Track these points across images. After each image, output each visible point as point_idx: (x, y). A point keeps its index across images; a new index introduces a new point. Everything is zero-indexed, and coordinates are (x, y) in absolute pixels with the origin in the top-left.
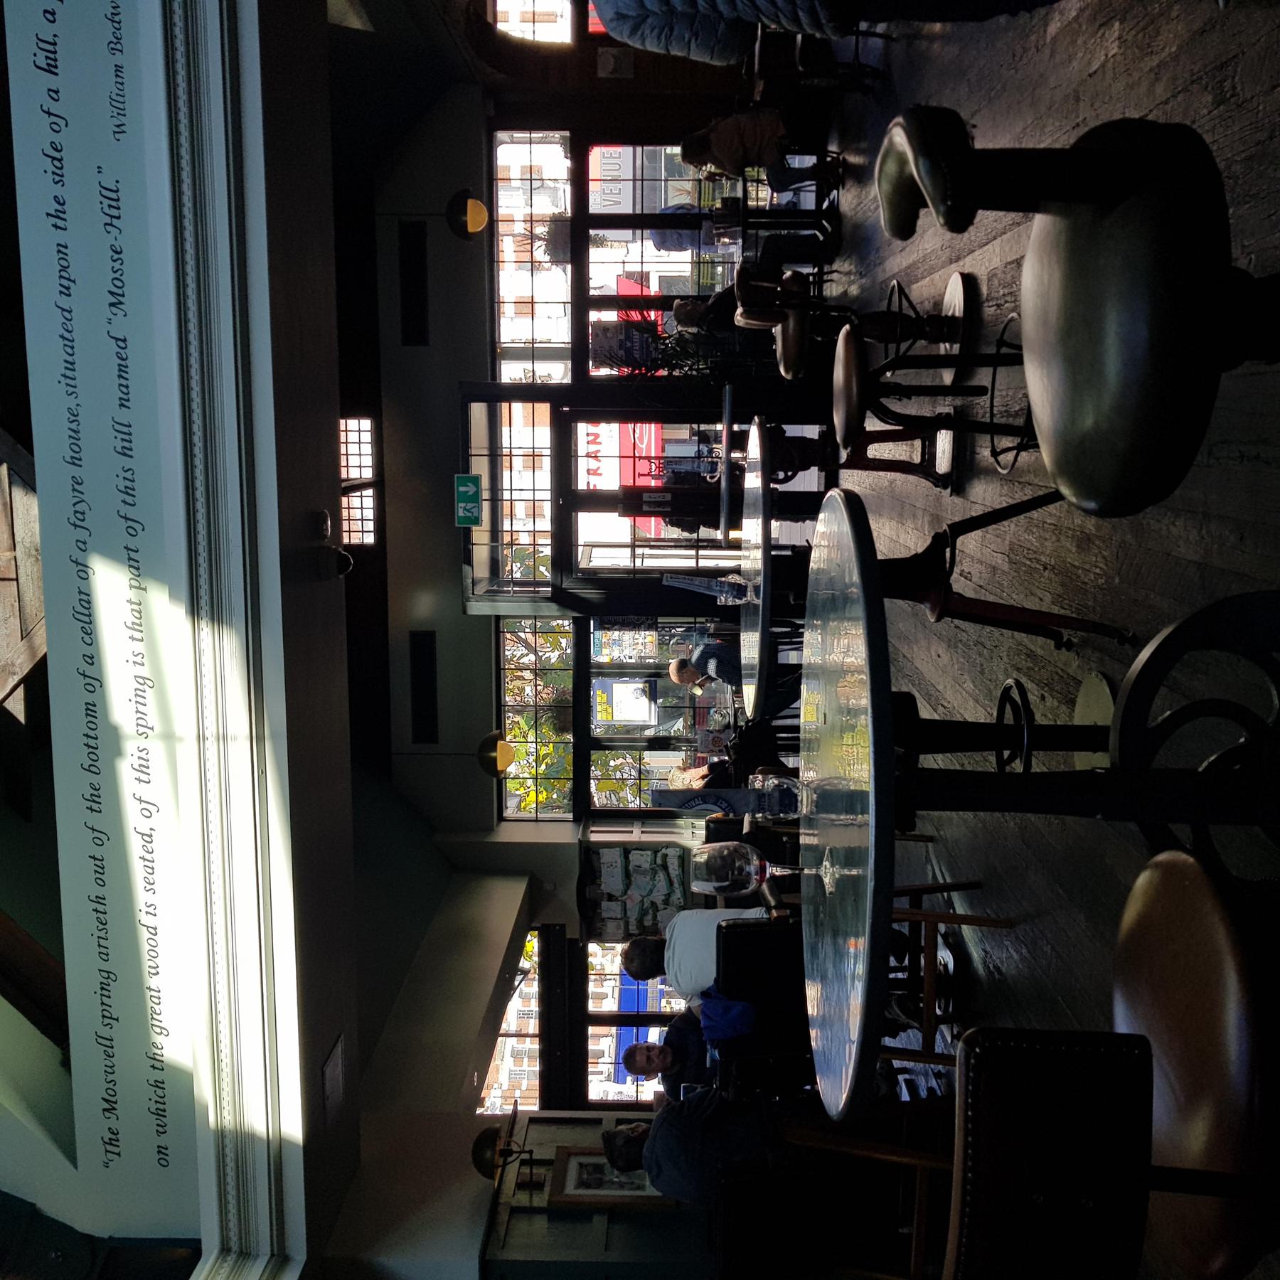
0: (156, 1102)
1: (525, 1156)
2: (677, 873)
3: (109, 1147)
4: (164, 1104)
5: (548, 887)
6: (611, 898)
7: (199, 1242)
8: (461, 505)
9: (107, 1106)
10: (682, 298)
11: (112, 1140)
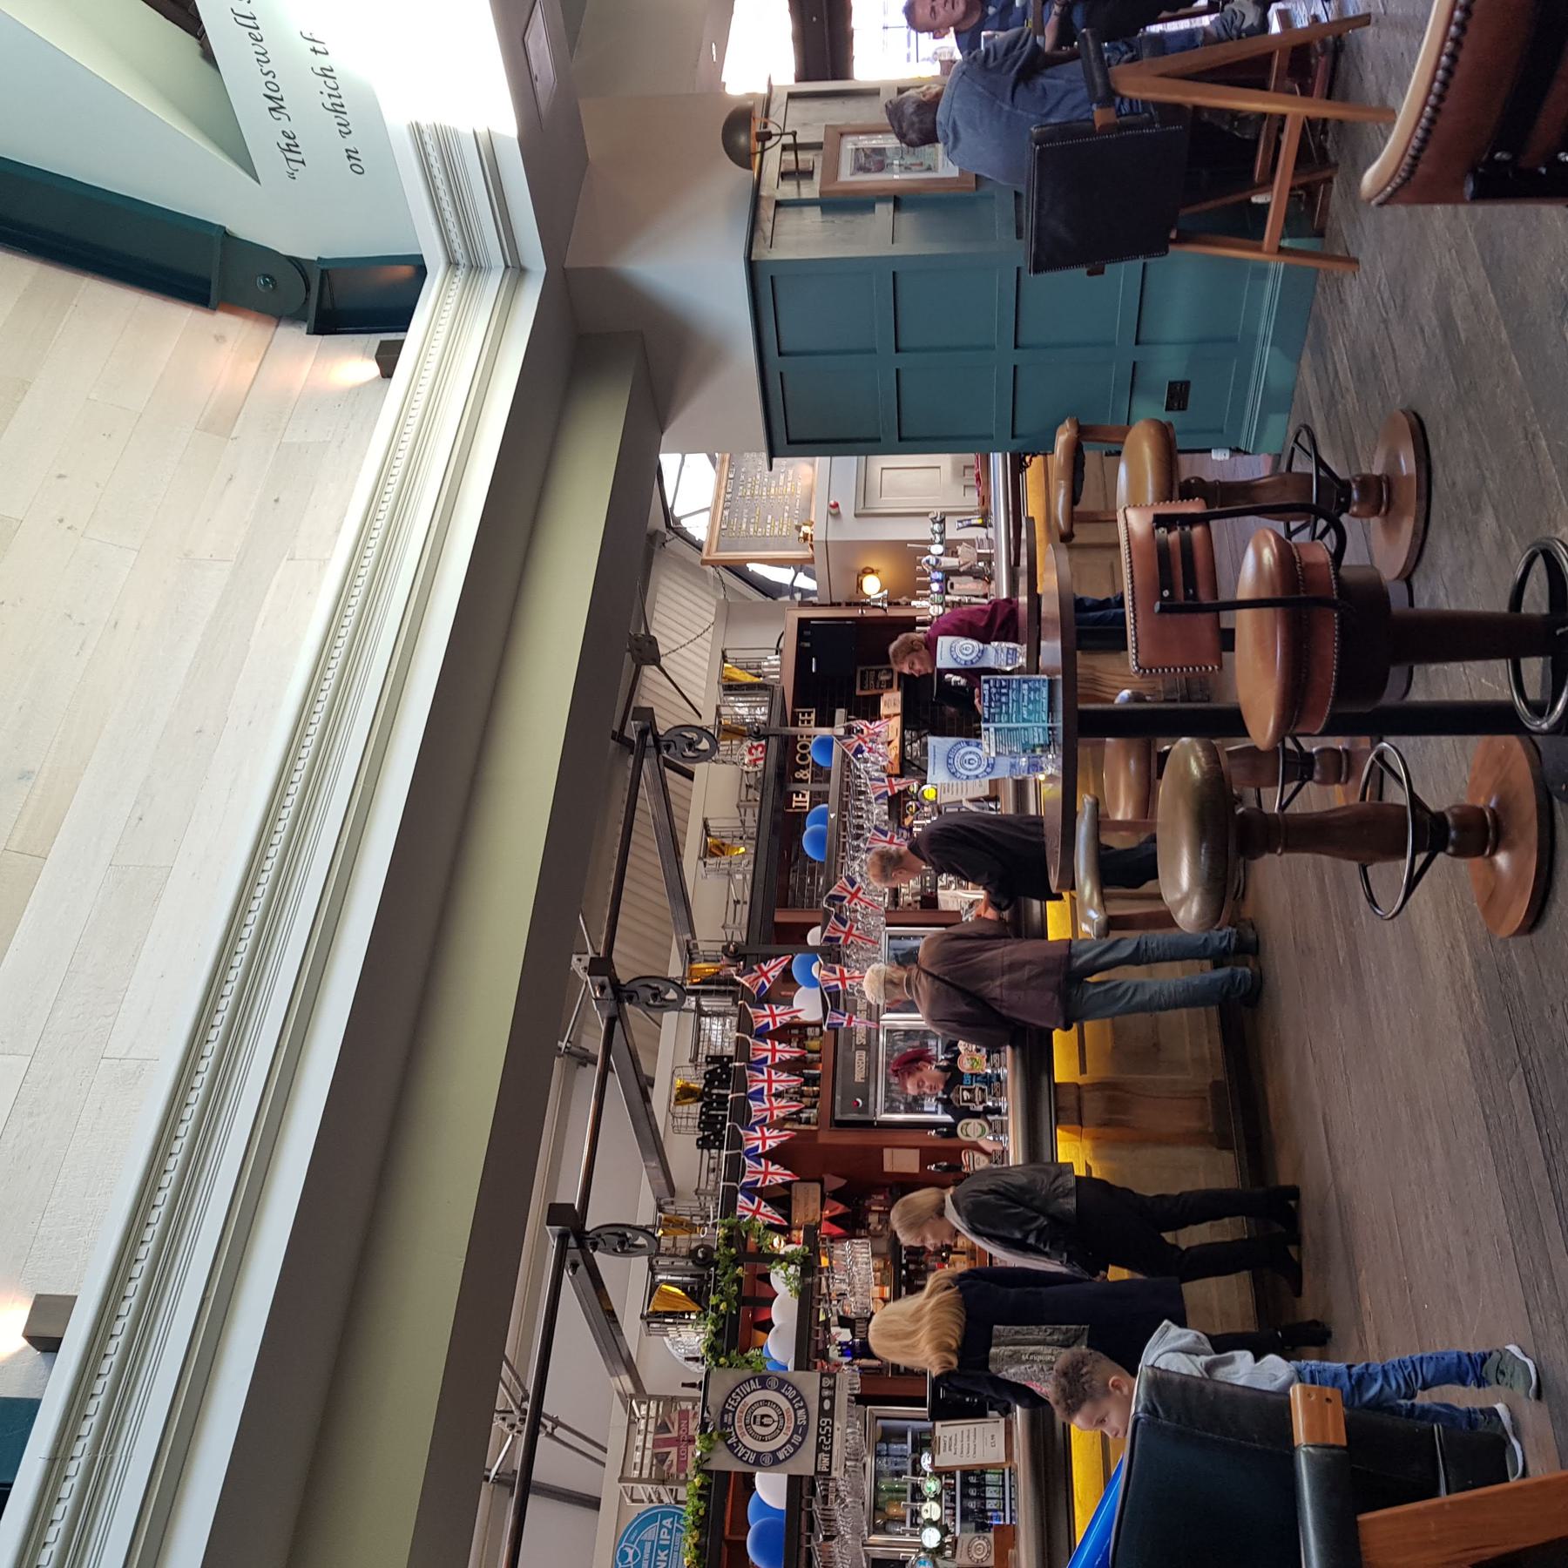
0: (330, 95)
1: (788, 140)
3: (289, 155)
4: (340, 97)
7: (422, 256)
9: (273, 105)
11: (291, 147)
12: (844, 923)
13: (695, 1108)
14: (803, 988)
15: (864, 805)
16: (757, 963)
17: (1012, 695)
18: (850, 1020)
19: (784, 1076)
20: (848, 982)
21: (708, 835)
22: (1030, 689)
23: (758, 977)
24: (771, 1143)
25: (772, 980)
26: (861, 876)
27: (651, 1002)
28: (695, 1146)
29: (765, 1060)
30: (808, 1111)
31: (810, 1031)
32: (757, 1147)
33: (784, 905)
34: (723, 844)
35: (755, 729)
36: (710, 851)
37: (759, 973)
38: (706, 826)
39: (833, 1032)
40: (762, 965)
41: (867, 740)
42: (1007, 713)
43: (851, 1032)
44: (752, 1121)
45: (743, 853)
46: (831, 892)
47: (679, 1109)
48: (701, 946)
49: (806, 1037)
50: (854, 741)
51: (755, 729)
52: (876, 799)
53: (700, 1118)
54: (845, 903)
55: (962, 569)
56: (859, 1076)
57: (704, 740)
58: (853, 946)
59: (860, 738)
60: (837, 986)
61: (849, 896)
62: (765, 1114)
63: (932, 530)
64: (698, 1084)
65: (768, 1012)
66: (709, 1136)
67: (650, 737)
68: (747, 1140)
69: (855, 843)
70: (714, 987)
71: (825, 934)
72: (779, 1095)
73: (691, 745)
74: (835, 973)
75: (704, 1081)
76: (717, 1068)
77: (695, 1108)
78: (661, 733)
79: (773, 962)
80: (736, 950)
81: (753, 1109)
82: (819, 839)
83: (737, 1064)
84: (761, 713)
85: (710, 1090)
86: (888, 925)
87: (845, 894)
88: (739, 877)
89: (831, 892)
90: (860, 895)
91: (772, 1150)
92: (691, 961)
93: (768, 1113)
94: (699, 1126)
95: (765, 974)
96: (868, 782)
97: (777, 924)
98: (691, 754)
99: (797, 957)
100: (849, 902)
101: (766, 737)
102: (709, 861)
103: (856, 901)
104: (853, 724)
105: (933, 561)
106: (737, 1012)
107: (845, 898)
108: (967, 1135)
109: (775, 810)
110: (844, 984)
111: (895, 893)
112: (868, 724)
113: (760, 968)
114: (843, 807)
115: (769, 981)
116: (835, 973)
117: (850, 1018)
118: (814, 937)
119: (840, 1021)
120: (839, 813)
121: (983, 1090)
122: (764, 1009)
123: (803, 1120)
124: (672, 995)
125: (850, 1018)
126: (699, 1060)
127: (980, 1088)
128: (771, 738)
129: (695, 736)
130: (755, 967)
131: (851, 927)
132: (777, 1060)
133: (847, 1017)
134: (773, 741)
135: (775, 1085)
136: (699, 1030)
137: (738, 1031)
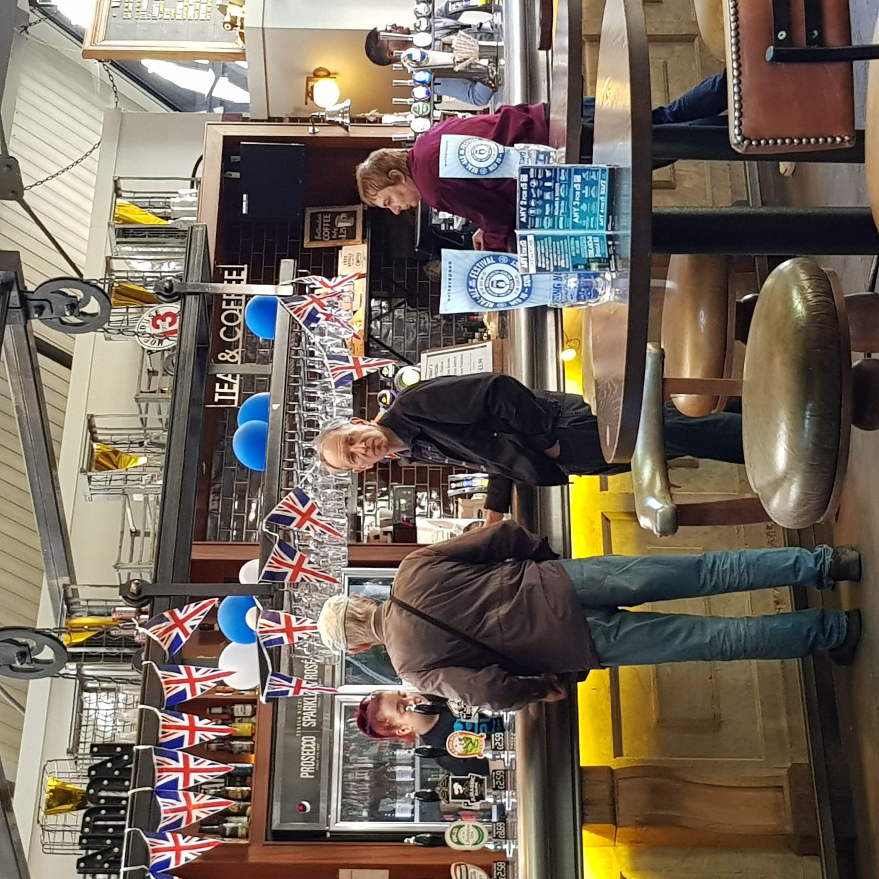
12: (291, 554)
13: (76, 818)
14: (234, 644)
15: (319, 394)
16: (170, 608)
17: (560, 191)
18: (298, 687)
19: (206, 764)
20: (296, 635)
21: (94, 439)
22: (584, 183)
23: (171, 628)
24: (188, 856)
25: (190, 631)
26: (316, 490)
27: (18, 664)
28: (76, 870)
29: (179, 741)
30: (234, 819)
31: (238, 709)
32: (167, 862)
33: (202, 536)
34: (116, 453)
35: (167, 284)
36: (98, 462)
37: (172, 622)
38: (91, 427)
39: (271, 704)
40: (177, 611)
41: (325, 302)
42: (552, 215)
43: (294, 704)
44: (161, 826)
45: (144, 466)
46: (274, 512)
47: (51, 820)
48: (84, 593)
49: (233, 718)
50: (307, 304)
51: (167, 284)
52: (337, 384)
53: (82, 832)
54: (293, 526)
55: (457, 69)
56: (305, 772)
57: (93, 300)
58: (303, 586)
59: (314, 300)
60: (281, 640)
61: (298, 518)
62: (180, 815)
63: (416, 12)
64: (80, 785)
65: (185, 676)
66: (95, 855)
67: (14, 293)
68: (155, 851)
69: (306, 445)
70: (103, 650)
71: (266, 569)
72: (197, 789)
73: (74, 306)
74: (279, 622)
75: (87, 781)
76: (106, 762)
77: (76, 818)
78: (31, 288)
79: (192, 608)
80: (139, 591)
81: (163, 808)
82: (257, 441)
83: (141, 747)
84: (172, 267)
85: (96, 792)
86: (351, 564)
87: (293, 514)
88: (138, 497)
89: (274, 512)
90: (314, 516)
91: (189, 866)
92: (70, 613)
93: (184, 814)
94: (80, 843)
95: (179, 624)
96: (326, 361)
97: (194, 562)
98: (74, 320)
99: (228, 598)
100: (299, 526)
101: (180, 297)
102: (97, 476)
103: (308, 523)
104: (305, 280)
105: (416, 55)
106: (141, 677)
107: (293, 519)
108: (459, 843)
109: (193, 402)
110: (290, 637)
111: (356, 523)
112: (326, 280)
113: (173, 615)
114: (291, 397)
115: (186, 633)
116: (279, 622)
117: (299, 683)
118: (250, 574)
119: (284, 689)
120: (285, 404)
121: (480, 782)
122: (180, 673)
123: (228, 832)
124: (47, 654)
125: (299, 683)
126: (81, 751)
127: (477, 780)
128: (188, 298)
129: (80, 294)
130: (167, 614)
131: (302, 559)
132: (197, 742)
133: (294, 684)
134: (192, 303)
135: (193, 776)
136: (81, 709)
137: (142, 703)
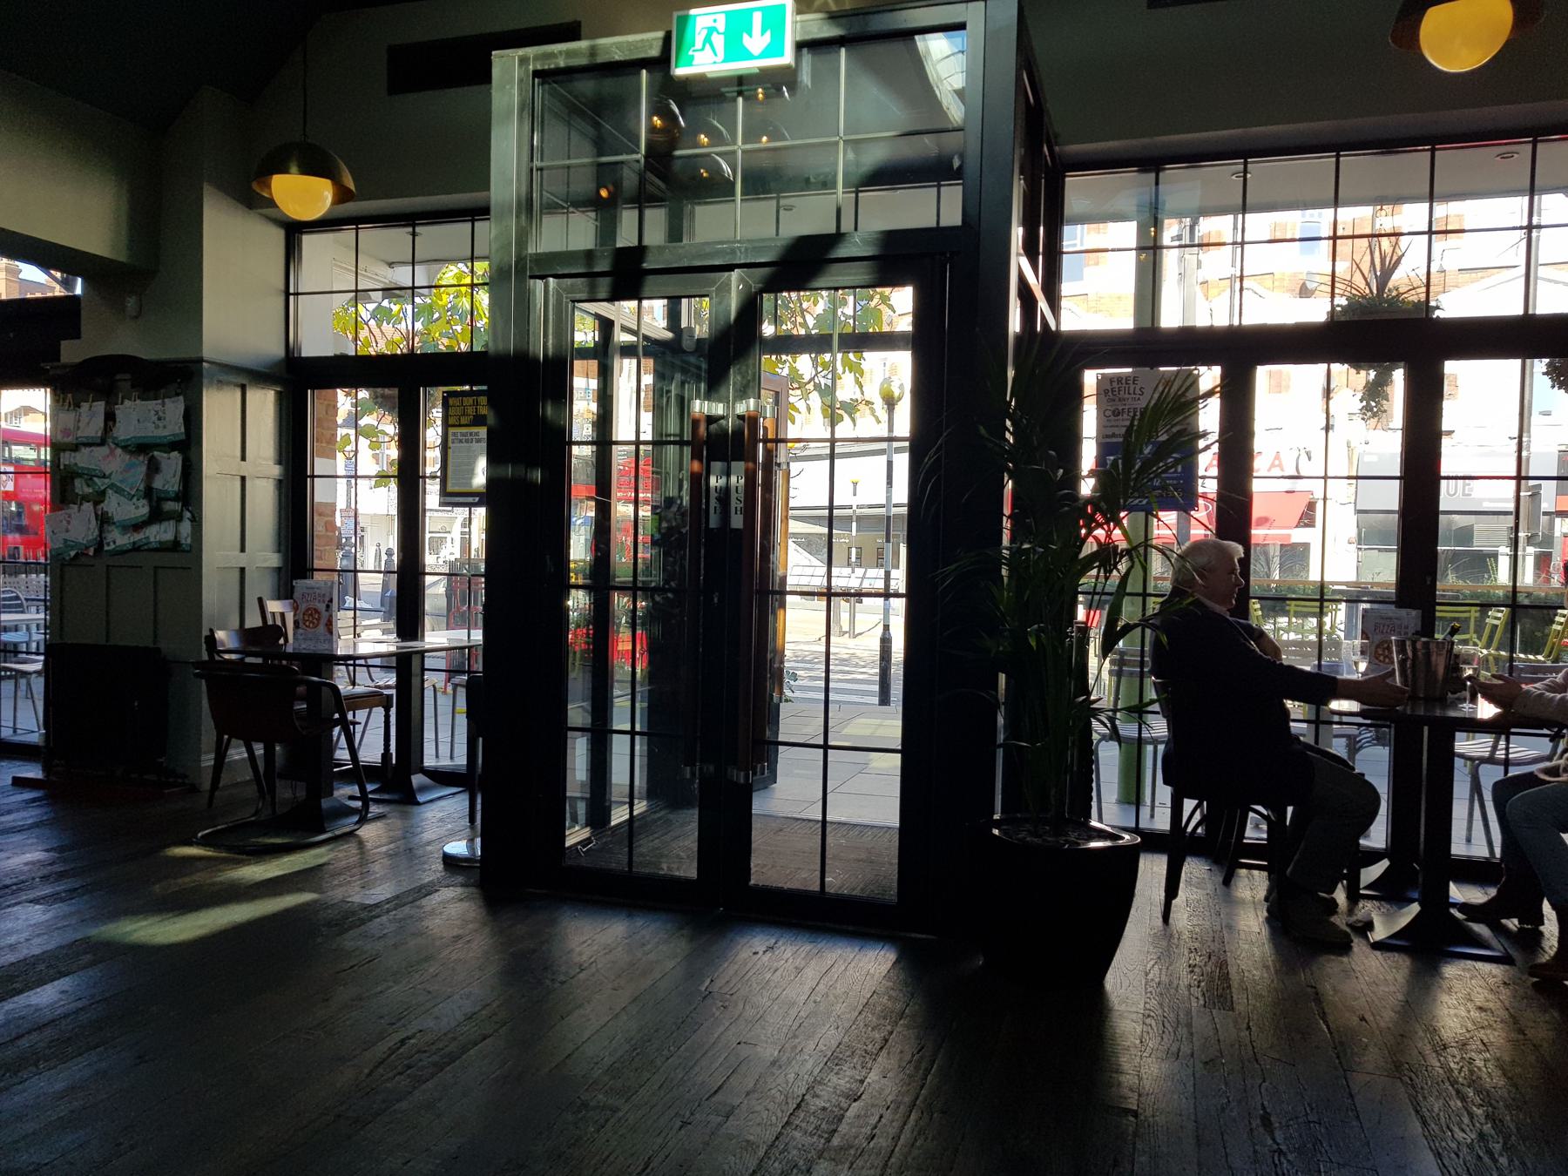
2: (152, 540)
5: (131, 302)
6: (110, 417)
8: (722, 19)
10: (1245, 562)
